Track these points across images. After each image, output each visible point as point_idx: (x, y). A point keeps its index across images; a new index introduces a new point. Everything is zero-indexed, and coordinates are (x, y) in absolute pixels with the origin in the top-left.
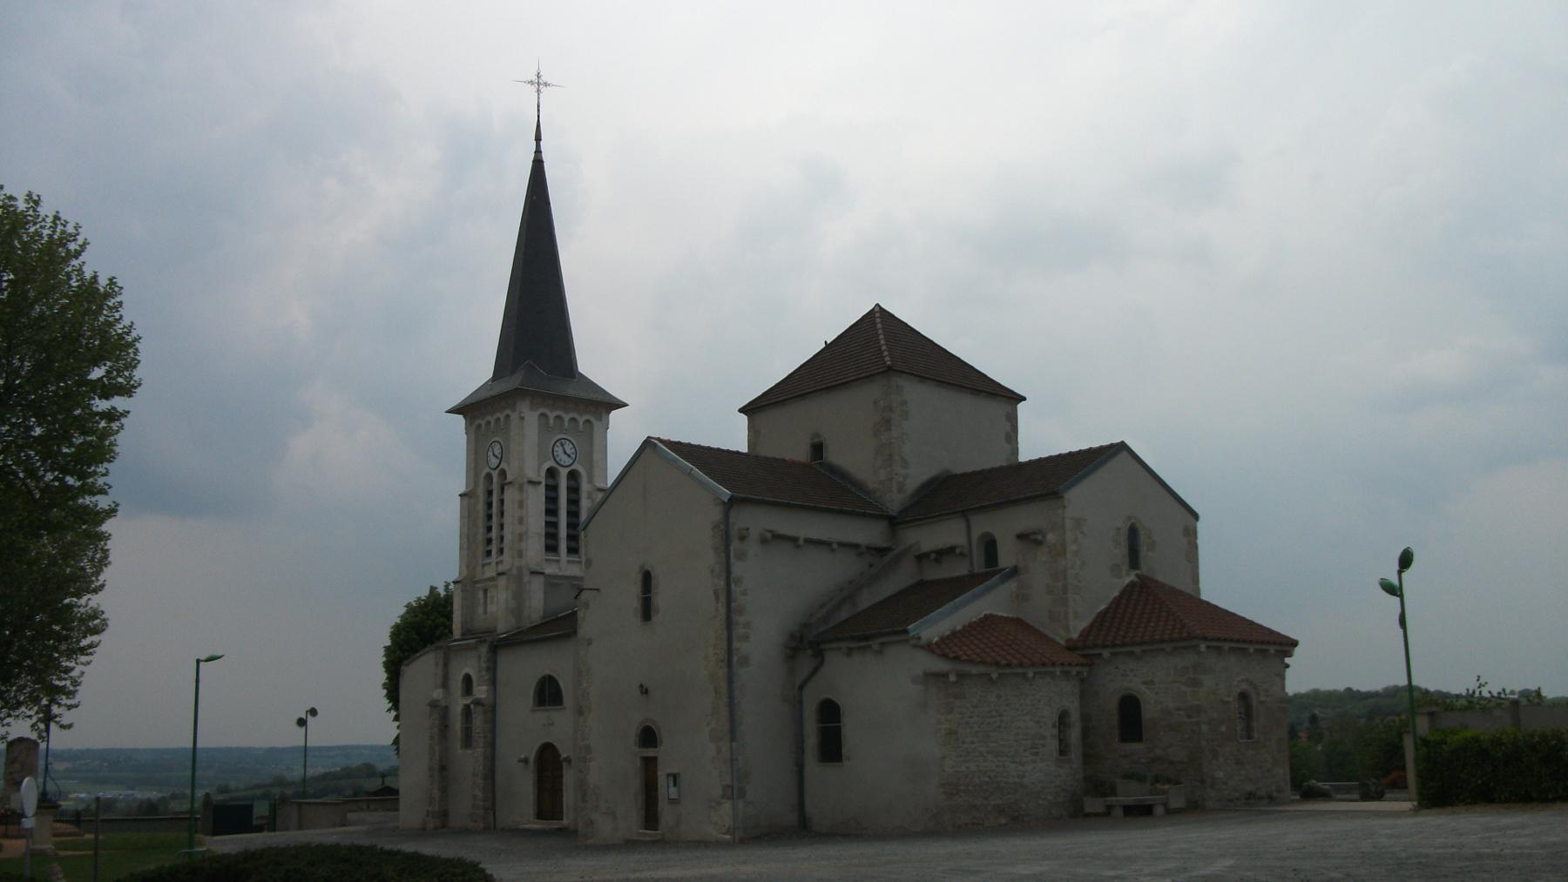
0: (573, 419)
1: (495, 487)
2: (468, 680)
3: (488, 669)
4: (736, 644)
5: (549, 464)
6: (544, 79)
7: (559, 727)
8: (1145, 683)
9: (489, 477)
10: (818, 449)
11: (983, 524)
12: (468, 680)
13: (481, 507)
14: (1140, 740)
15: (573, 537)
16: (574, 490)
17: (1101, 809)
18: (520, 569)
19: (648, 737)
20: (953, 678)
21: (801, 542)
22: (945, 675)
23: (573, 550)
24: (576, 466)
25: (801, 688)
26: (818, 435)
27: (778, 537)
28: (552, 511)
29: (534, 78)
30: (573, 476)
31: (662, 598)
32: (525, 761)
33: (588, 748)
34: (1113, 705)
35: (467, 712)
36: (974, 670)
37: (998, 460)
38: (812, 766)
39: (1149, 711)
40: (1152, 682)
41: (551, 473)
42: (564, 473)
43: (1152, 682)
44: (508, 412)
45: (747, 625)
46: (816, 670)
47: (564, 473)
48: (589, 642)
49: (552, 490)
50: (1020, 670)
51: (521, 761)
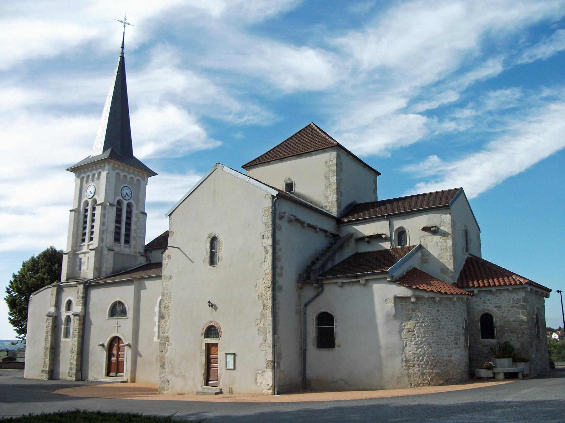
0: (132, 178)
1: (89, 208)
2: (69, 303)
3: (83, 297)
4: (277, 279)
5: (119, 198)
6: (127, 21)
7: (123, 328)
8: (496, 307)
9: (87, 203)
10: (290, 186)
11: (398, 224)
12: (69, 303)
13: (82, 217)
14: (493, 337)
15: (128, 235)
16: (129, 213)
17: (491, 375)
18: (102, 248)
19: (211, 331)
20: (413, 300)
21: (306, 225)
22: (409, 298)
23: (127, 242)
24: (131, 201)
25: (306, 305)
26: (289, 179)
27: (297, 220)
28: (118, 221)
29: (123, 20)
30: (129, 205)
31: (223, 253)
32: (103, 345)
33: (167, 338)
34: (478, 319)
35: (68, 318)
36: (426, 295)
37: (372, 200)
38: (313, 351)
39: (497, 323)
40: (500, 307)
41: (119, 203)
42: (125, 203)
43: (500, 307)
44: (100, 170)
45: (282, 268)
46: (317, 295)
47: (125, 203)
48: (170, 278)
49: (119, 211)
50: (451, 296)
51: (101, 345)
